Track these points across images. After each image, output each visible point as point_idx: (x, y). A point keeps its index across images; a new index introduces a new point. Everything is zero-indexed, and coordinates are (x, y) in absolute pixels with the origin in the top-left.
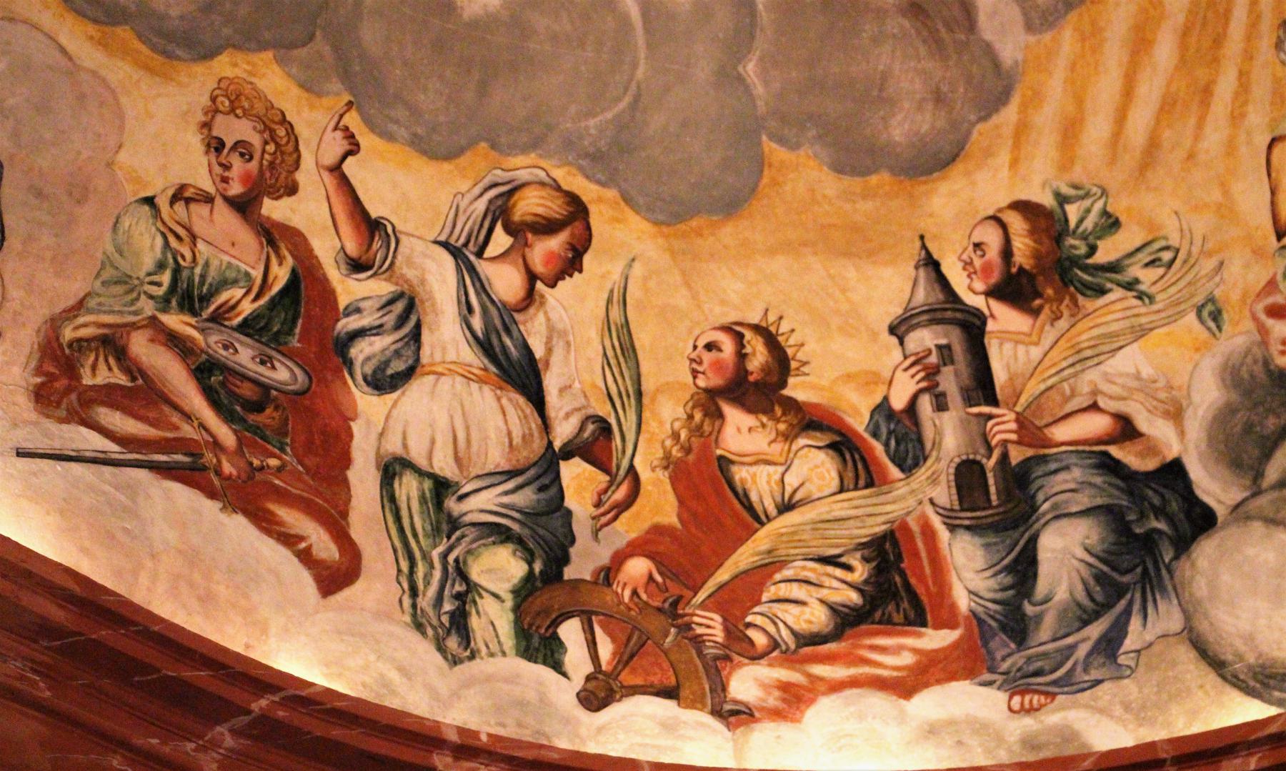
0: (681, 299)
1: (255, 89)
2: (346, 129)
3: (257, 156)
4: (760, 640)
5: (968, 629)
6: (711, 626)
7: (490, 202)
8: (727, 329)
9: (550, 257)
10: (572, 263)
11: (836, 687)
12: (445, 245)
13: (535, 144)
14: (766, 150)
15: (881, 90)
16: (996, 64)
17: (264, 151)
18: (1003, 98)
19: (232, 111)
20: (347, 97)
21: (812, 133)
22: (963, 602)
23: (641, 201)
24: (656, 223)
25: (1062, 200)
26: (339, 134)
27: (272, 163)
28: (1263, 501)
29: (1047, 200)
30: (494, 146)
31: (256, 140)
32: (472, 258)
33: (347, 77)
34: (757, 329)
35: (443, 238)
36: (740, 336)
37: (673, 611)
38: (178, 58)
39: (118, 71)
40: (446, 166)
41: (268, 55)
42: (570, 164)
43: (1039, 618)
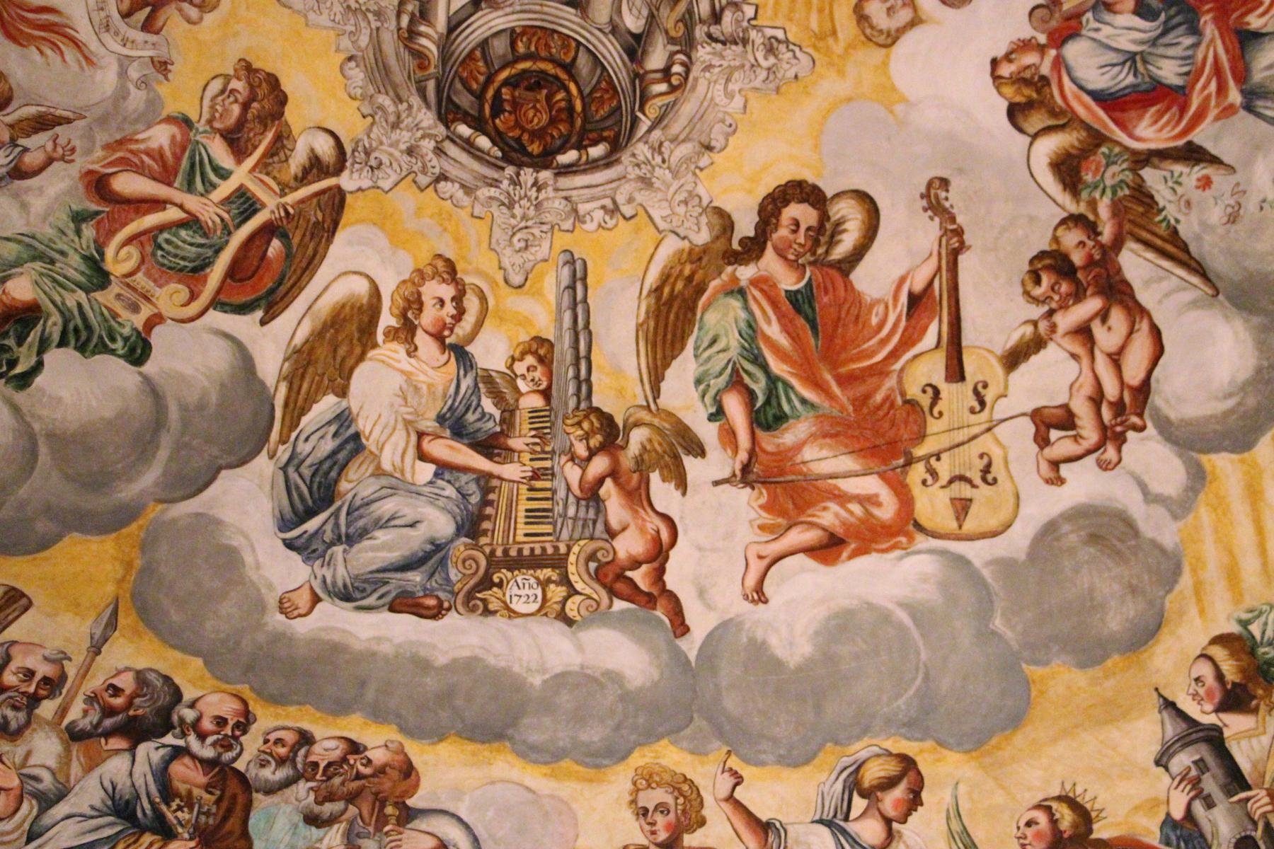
0: (999, 798)
1: (661, 766)
2: (731, 769)
3: (672, 809)
7: (845, 781)
8: (1038, 807)
9: (897, 803)
10: (915, 801)
12: (821, 822)
13: (866, 731)
14: (1027, 671)
15: (1092, 599)
16: (1163, 551)
17: (676, 804)
18: (1177, 571)
19: (649, 786)
20: (725, 749)
21: (1056, 648)
23: (951, 741)
24: (967, 752)
25: (1245, 624)
26: (726, 775)
27: (684, 811)
29: (1235, 628)
30: (837, 743)
31: (669, 799)
32: (842, 823)
33: (721, 734)
34: (1060, 798)
35: (817, 817)
36: (1049, 809)
38: (606, 766)
39: (566, 789)
40: (807, 769)
41: (665, 742)
42: (895, 735)
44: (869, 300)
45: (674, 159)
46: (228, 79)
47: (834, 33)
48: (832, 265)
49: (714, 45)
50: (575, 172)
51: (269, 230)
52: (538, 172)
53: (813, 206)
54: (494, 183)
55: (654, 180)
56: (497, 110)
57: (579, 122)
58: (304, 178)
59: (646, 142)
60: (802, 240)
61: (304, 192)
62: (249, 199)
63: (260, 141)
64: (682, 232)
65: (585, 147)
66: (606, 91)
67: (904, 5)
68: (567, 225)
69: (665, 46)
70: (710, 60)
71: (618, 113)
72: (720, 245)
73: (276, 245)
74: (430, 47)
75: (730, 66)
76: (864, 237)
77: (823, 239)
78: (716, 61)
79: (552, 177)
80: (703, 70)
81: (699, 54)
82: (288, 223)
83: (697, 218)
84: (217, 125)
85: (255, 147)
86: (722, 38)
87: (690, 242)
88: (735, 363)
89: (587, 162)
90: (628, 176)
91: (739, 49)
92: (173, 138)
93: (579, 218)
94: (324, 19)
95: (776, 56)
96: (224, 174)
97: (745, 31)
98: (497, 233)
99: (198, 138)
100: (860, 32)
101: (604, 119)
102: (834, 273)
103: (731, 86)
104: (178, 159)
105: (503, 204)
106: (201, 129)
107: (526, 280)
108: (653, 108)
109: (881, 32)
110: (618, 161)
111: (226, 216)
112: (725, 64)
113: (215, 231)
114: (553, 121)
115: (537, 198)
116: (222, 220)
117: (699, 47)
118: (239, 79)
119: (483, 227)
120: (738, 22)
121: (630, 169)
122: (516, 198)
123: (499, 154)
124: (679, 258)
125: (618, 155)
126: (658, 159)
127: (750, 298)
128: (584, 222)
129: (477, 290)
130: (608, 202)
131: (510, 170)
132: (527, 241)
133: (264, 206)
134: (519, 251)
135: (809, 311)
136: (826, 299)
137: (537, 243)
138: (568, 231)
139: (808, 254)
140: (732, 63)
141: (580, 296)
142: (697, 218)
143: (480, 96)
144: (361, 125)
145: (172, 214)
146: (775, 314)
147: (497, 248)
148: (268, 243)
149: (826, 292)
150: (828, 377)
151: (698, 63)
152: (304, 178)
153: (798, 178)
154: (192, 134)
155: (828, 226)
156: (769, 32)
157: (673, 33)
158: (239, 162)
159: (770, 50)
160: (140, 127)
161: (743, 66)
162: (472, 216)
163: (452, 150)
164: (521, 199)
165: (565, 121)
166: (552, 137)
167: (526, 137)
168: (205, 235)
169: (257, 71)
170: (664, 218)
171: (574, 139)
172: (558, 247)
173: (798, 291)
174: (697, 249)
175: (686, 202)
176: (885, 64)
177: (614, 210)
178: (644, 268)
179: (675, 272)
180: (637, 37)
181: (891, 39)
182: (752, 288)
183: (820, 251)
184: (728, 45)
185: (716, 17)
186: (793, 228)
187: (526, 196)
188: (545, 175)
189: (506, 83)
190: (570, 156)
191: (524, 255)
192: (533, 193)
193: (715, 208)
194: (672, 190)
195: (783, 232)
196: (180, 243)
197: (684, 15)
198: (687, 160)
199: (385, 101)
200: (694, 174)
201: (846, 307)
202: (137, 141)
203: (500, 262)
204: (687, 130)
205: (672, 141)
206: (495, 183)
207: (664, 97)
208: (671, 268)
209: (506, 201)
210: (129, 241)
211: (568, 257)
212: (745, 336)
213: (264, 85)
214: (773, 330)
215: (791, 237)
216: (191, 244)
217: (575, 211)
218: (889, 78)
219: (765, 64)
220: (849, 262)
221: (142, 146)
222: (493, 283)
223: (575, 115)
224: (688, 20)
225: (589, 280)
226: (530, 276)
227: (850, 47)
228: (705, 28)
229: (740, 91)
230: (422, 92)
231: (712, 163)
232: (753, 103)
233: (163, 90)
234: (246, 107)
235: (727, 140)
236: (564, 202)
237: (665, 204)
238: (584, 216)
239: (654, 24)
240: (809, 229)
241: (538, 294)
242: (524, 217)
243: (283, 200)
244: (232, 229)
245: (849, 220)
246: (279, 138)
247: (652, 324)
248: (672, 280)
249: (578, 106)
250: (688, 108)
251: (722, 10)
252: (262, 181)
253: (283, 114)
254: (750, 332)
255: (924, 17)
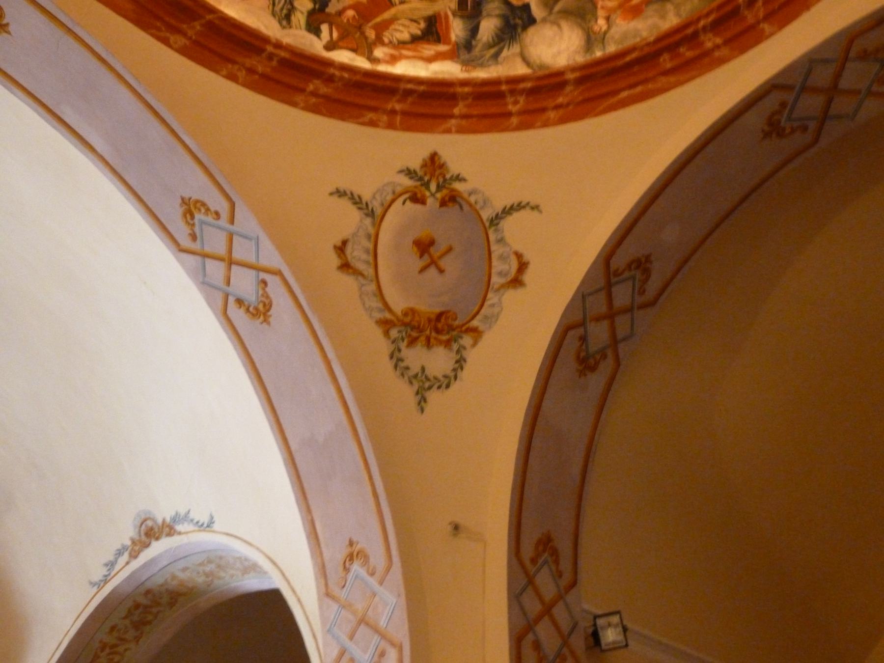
4: (386, 40)
5: (454, 46)
6: (371, 34)
11: (408, 57)
22: (453, 38)
28: (552, 17)
37: (360, 28)
43: (476, 46)
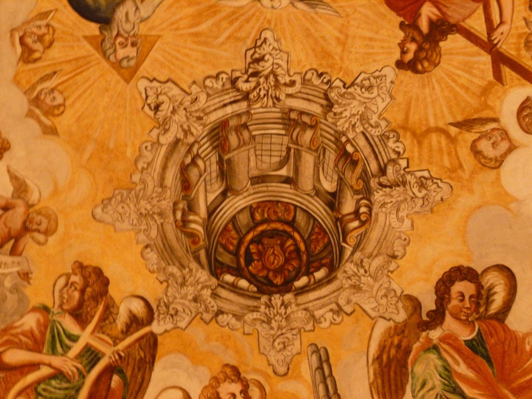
44: (521, 335)
45: (372, 270)
46: (68, 276)
47: (461, 166)
48: (492, 317)
49: (384, 189)
50: (308, 291)
51: (110, 370)
52: (283, 296)
53: (470, 281)
54: (255, 309)
55: (362, 285)
56: (249, 260)
57: (304, 258)
58: (128, 330)
59: (352, 262)
60: (468, 305)
61: (129, 340)
62: (93, 352)
63: (95, 313)
64: (387, 316)
65: (312, 273)
66: (319, 234)
67: (502, 139)
68: (309, 327)
69: (352, 197)
70: (383, 200)
71: (329, 248)
72: (415, 320)
73: (116, 379)
74: (198, 228)
75: (397, 201)
76: (509, 294)
77: (482, 302)
78: (388, 200)
79: (293, 297)
80: (380, 207)
81: (376, 197)
82: (122, 362)
83: (395, 304)
84: (66, 307)
85: (93, 317)
86: (389, 184)
87: (394, 321)
88: (441, 396)
89: (315, 283)
90: (344, 286)
91: (401, 189)
92: (38, 321)
93: (316, 321)
94: (126, 225)
95: (426, 189)
96: (74, 339)
97: (403, 176)
98: (262, 341)
99: (55, 318)
100: (477, 162)
101: (321, 252)
102: (495, 323)
103: (400, 214)
104: (43, 334)
105: (263, 322)
106: (56, 312)
107: (288, 369)
108: (352, 238)
109: (491, 159)
110: (335, 278)
111: (80, 366)
112: (394, 200)
113: (74, 377)
114: (287, 261)
115: (285, 313)
116: (78, 369)
117: (375, 193)
118: (75, 274)
119: (253, 340)
120: (397, 171)
121: (344, 281)
122: (272, 316)
123: (255, 289)
124: (389, 334)
125: (335, 274)
126: (362, 271)
127: (441, 350)
128: (320, 323)
129: (256, 383)
130: (334, 306)
131: (264, 299)
132: (284, 343)
133: (104, 354)
134: (280, 350)
135: (483, 351)
136: (492, 341)
137: (291, 343)
138: (310, 331)
139: (474, 313)
140: (399, 199)
141: (327, 372)
142: (395, 304)
143: (236, 254)
144: (160, 289)
145: (45, 371)
146: (460, 357)
147: (265, 352)
148: (111, 379)
149: (492, 336)
150: (506, 392)
151: (376, 203)
152: (128, 330)
153: (456, 264)
154: (50, 317)
155: (483, 292)
156: (419, 174)
157: (356, 188)
158: (83, 328)
159: (422, 186)
160: (16, 317)
161: (406, 199)
162: (244, 333)
163: (224, 293)
164: (275, 316)
165: (295, 259)
166: (289, 271)
167: (271, 274)
168: (68, 381)
169: (86, 267)
170: (373, 309)
171: (303, 269)
172: (305, 343)
173: (473, 340)
174: (399, 325)
175: (386, 296)
176: (498, 179)
177: (339, 311)
178: (366, 345)
179: (388, 343)
180: (333, 195)
181: (499, 162)
182: (442, 344)
183: (482, 310)
184: (394, 188)
185: (383, 171)
186: (460, 298)
187: (278, 313)
188: (288, 297)
189: (252, 242)
190: (303, 281)
191: (284, 353)
192: (282, 310)
193: (406, 295)
194: (375, 289)
195: (455, 302)
196: (52, 390)
197: (361, 174)
198: (381, 268)
199: (174, 269)
200: (388, 276)
201: (508, 342)
202: (16, 328)
203: (268, 361)
204: (377, 249)
205: (369, 257)
206: (255, 309)
207: (358, 230)
208: (385, 341)
209: (265, 319)
210: (19, 394)
211: (314, 348)
212: (444, 376)
213: (93, 275)
214: (462, 369)
215: (460, 304)
216: (60, 389)
217: (313, 316)
218: (502, 188)
219: (420, 195)
220: (503, 313)
221: (19, 330)
222: (266, 376)
223: (302, 254)
224: (365, 177)
225: (331, 361)
226: (290, 366)
227: (473, 173)
228: (377, 180)
229: (407, 216)
230: (197, 259)
231: (398, 267)
232: (418, 223)
233: (28, 291)
234: (83, 292)
235: (405, 250)
236: (304, 312)
237: (372, 300)
238: (320, 319)
239: (343, 184)
240: (471, 297)
241: (299, 377)
242: (280, 328)
243: (116, 348)
244: (85, 374)
245: (497, 285)
246: (107, 308)
247: (379, 381)
248: (387, 349)
249: (302, 246)
250: (375, 234)
251: (386, 166)
252: (100, 338)
253: (107, 292)
254: (447, 373)
255: (516, 145)
